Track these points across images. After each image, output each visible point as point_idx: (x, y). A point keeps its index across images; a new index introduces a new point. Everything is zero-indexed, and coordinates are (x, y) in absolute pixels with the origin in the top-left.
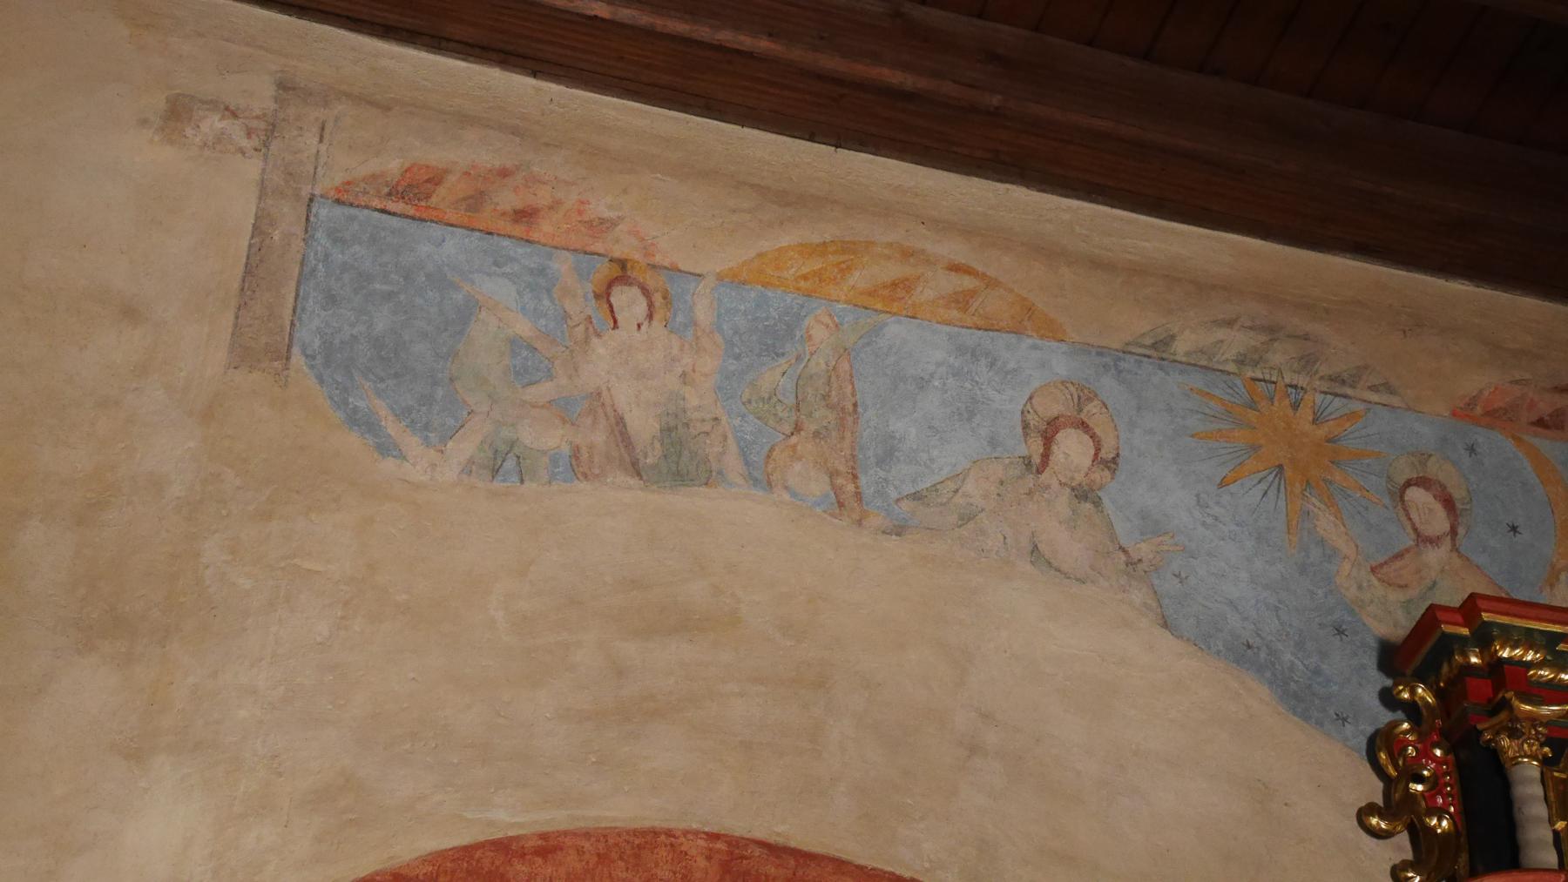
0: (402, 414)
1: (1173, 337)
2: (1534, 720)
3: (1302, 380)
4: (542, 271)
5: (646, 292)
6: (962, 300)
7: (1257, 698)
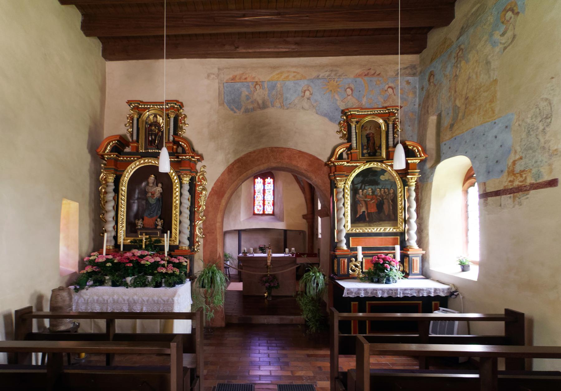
0: (236, 108)
1: (319, 75)
2: (354, 121)
3: (335, 77)
4: (248, 85)
5: (259, 85)
6: (294, 77)
7: (326, 120)
